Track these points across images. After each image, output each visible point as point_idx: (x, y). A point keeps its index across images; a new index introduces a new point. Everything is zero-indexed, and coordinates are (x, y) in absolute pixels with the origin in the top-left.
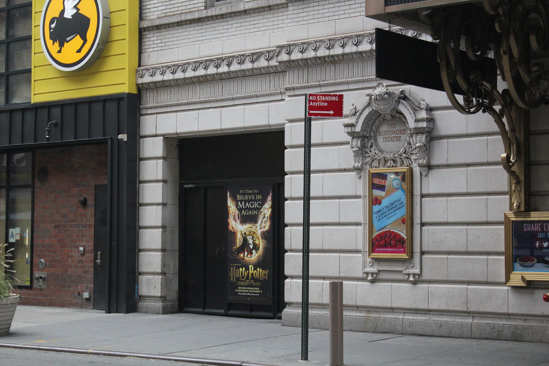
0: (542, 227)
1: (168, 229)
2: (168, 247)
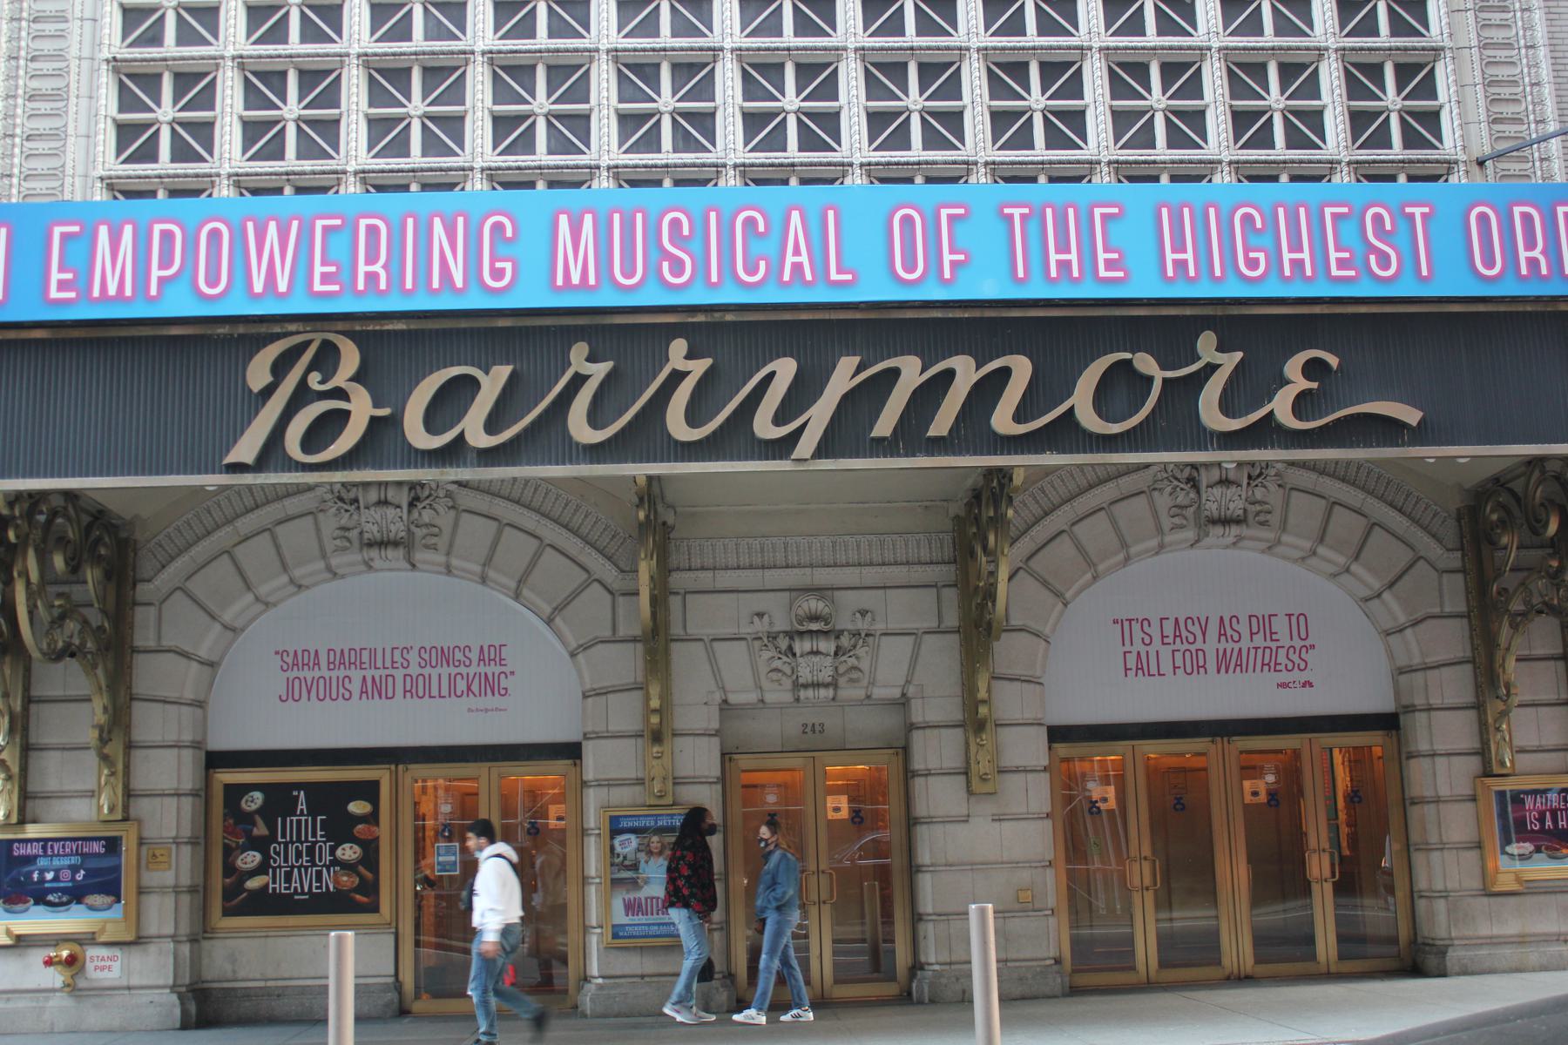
0: (44, 848)
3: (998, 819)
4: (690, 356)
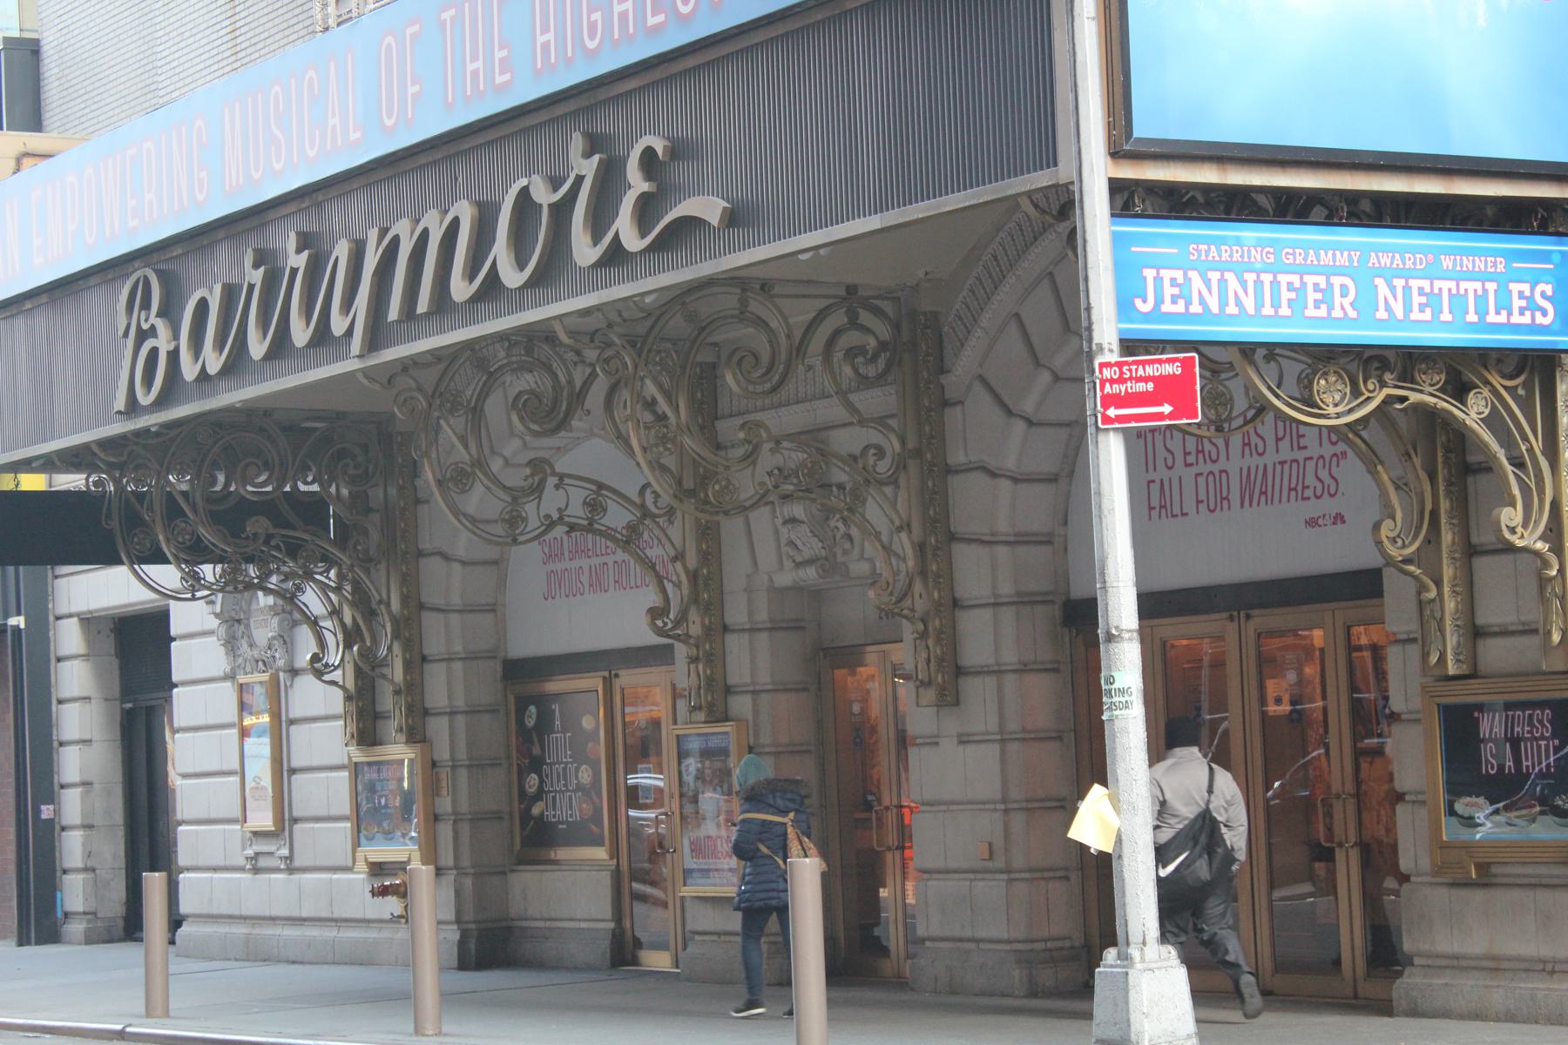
1: (96, 786)
2: (98, 820)
3: (963, 740)
4: (299, 251)
